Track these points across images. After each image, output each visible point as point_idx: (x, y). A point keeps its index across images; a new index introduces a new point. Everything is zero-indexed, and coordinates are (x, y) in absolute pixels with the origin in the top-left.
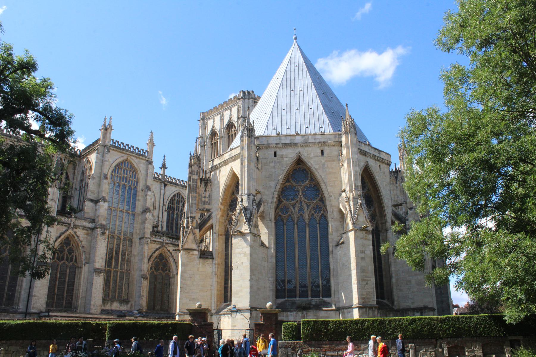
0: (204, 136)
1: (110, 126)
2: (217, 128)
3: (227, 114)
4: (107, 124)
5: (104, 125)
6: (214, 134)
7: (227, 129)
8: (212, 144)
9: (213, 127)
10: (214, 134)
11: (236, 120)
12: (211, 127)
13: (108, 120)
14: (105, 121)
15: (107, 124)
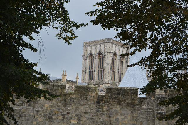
0: (85, 55)
1: (66, 74)
2: (94, 52)
3: (98, 46)
4: (64, 73)
5: (63, 74)
6: (91, 55)
7: (98, 55)
8: (90, 60)
9: (91, 51)
10: (91, 55)
11: (103, 52)
12: (90, 51)
13: (64, 71)
14: (63, 72)
15: (64, 73)
